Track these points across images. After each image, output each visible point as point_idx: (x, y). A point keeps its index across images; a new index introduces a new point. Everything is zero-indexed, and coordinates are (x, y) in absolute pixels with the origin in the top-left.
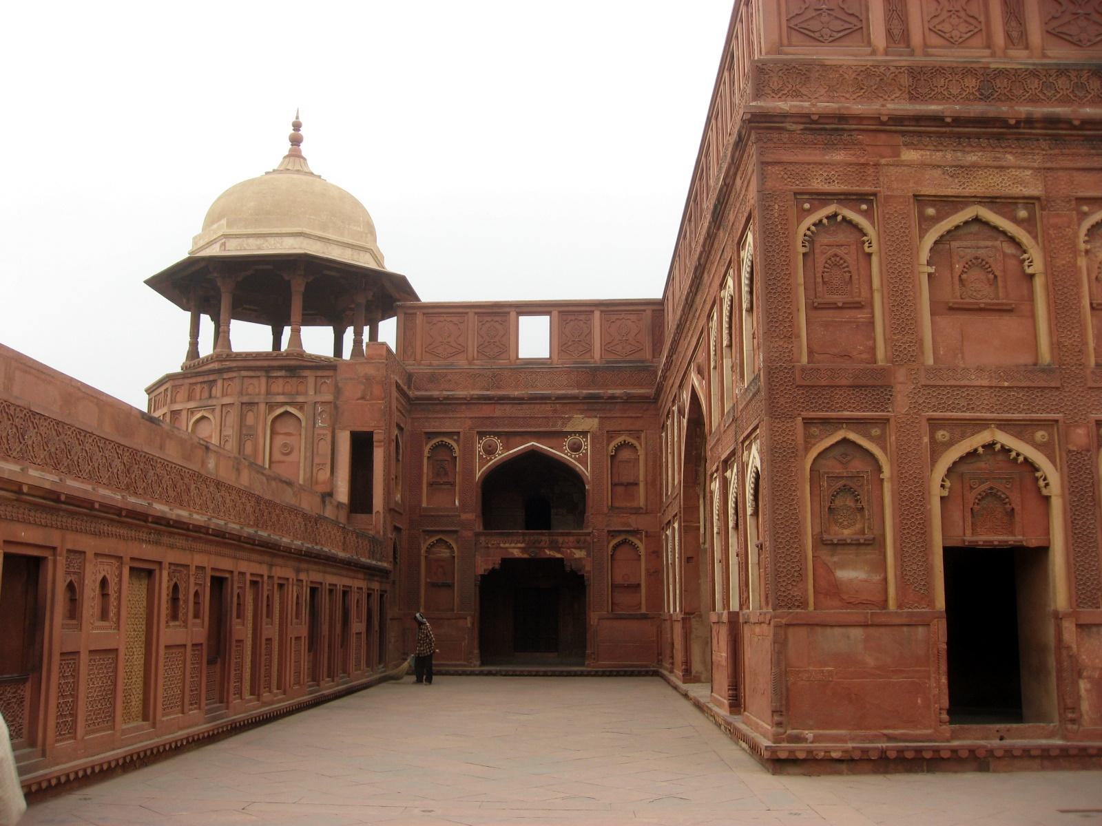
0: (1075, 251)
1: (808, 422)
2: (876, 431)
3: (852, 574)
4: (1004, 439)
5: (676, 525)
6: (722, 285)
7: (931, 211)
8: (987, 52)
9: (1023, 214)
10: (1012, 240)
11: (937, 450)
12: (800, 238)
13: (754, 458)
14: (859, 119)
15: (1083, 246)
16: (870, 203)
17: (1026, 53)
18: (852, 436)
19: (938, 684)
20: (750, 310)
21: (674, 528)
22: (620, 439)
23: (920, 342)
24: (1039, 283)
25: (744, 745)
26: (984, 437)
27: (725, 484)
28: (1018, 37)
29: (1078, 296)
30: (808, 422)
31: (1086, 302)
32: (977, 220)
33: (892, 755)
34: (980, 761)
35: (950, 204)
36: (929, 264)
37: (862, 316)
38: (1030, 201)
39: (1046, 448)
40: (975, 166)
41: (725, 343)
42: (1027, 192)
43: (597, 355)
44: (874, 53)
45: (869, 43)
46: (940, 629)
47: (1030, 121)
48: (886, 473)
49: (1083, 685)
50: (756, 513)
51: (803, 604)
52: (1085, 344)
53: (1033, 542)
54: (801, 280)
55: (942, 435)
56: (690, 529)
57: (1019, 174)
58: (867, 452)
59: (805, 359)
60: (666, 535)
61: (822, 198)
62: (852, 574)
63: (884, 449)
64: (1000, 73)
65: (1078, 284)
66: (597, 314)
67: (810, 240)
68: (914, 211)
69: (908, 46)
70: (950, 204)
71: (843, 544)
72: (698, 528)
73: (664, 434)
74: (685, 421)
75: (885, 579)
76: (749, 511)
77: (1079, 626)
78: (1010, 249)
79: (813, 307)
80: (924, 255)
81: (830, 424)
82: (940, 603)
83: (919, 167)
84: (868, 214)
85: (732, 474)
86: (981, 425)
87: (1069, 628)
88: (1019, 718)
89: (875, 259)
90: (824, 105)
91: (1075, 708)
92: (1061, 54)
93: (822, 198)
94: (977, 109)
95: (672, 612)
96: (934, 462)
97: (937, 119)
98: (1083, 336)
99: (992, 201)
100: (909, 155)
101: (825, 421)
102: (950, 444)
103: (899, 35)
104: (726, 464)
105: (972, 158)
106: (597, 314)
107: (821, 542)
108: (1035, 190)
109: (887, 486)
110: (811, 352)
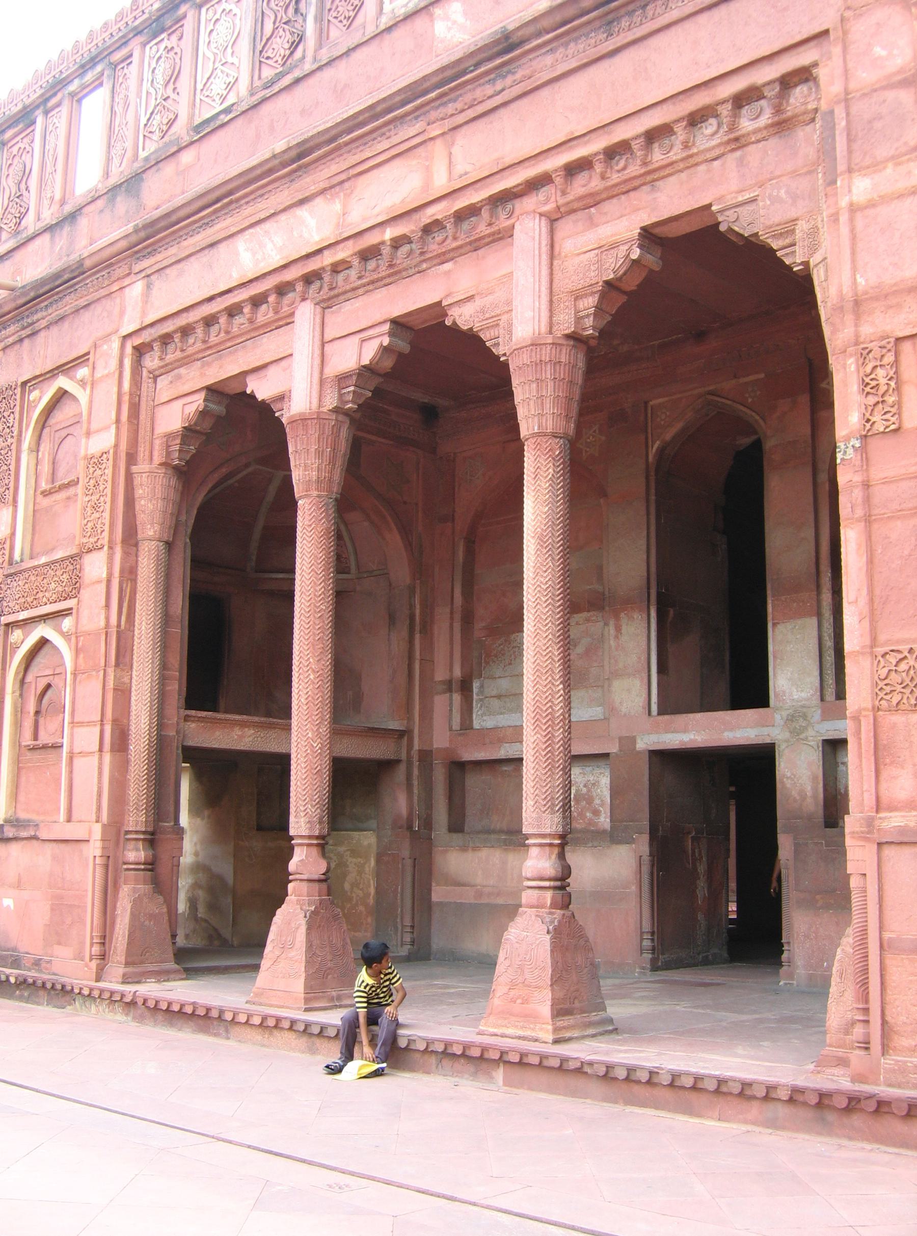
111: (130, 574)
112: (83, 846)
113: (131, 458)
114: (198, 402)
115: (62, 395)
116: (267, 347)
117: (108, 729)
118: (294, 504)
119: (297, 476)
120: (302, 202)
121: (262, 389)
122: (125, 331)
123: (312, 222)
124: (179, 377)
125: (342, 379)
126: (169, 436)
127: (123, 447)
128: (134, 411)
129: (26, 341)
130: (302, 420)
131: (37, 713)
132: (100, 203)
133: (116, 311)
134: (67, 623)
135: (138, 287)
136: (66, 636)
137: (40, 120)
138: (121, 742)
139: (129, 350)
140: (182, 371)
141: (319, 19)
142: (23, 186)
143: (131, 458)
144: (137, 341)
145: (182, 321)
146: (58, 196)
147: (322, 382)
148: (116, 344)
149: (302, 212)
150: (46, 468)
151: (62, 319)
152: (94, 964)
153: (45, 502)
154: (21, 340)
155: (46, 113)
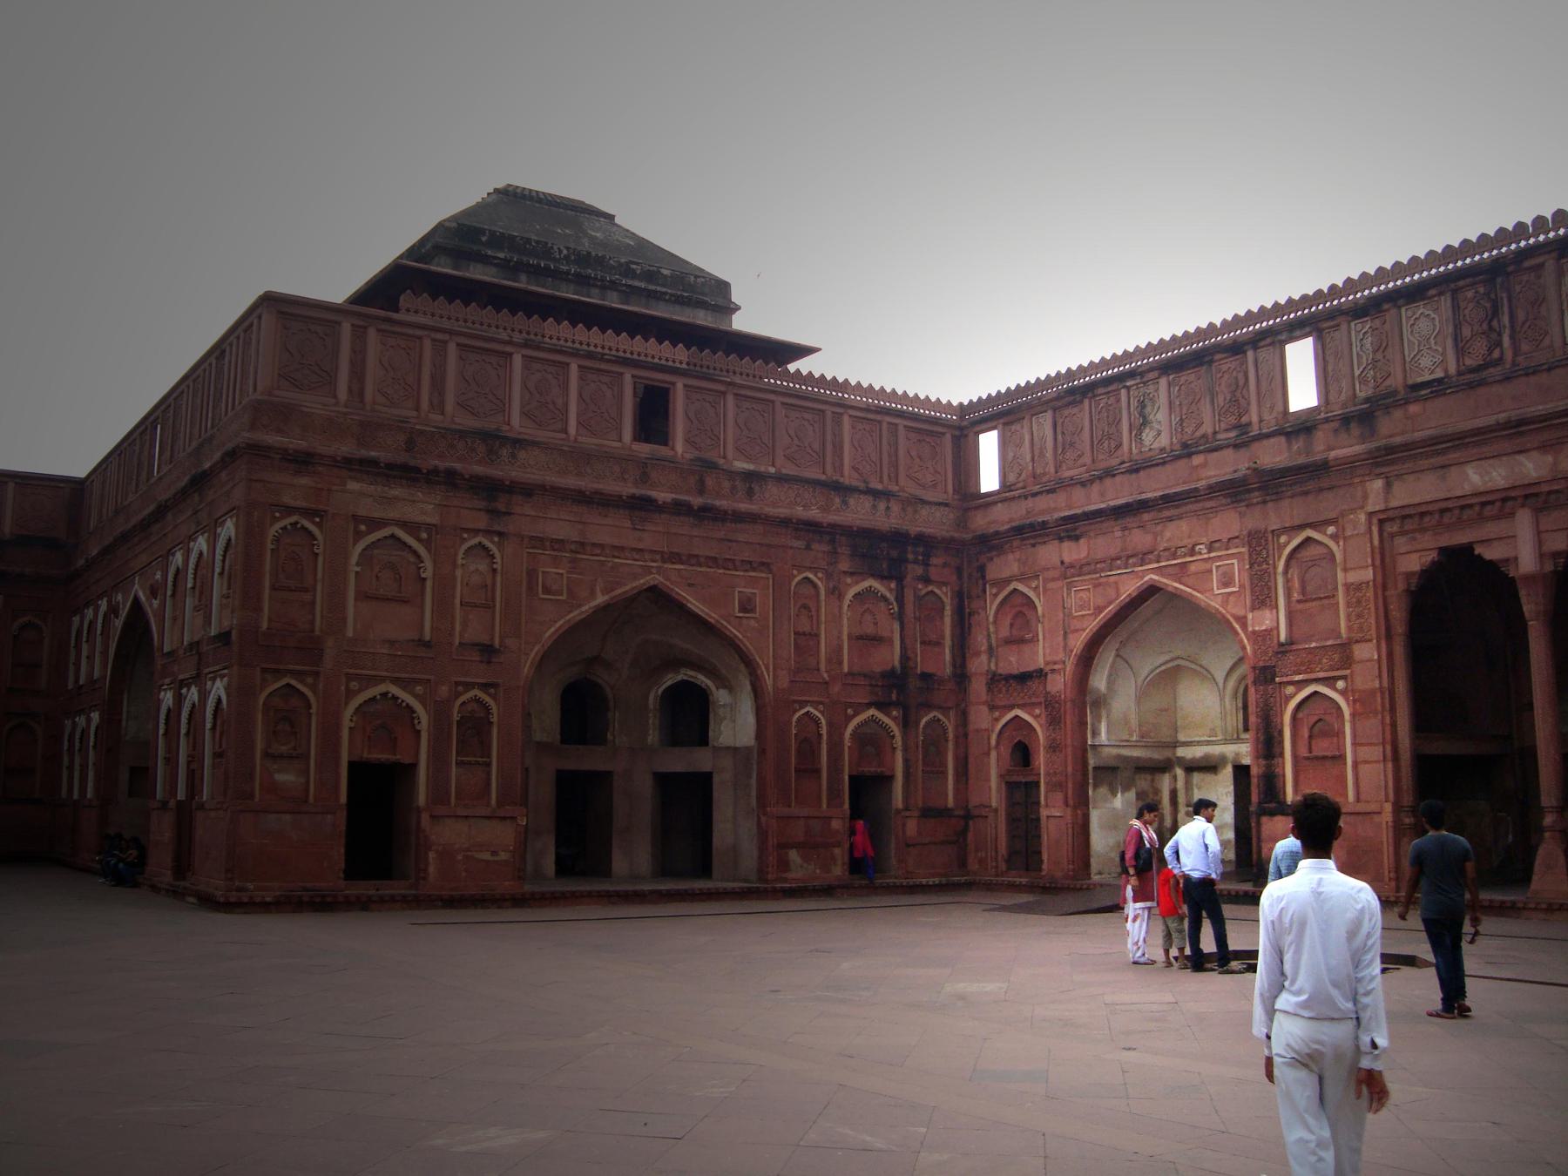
0: (454, 565)
1: (264, 670)
2: (310, 680)
3: (286, 777)
4: (395, 690)
5: (95, 716)
6: (192, 538)
7: (363, 528)
8: (414, 414)
9: (424, 535)
10: (415, 553)
11: (350, 694)
12: (270, 538)
13: (218, 689)
14: (322, 456)
15: (460, 562)
16: (321, 517)
17: (440, 417)
18: (293, 682)
19: (338, 853)
20: (221, 574)
21: (89, 720)
22: (26, 619)
23: (344, 620)
24: (429, 584)
25: (191, 899)
26: (382, 688)
27: (179, 699)
28: (439, 406)
29: (453, 596)
30: (264, 670)
31: (457, 601)
32: (393, 536)
33: (305, 899)
34: (364, 905)
35: (375, 524)
36: (358, 564)
37: (307, 597)
38: (429, 527)
39: (421, 699)
40: (396, 498)
41: (190, 585)
42: (429, 520)
43: (7, 530)
44: (337, 404)
45: (335, 397)
46: (342, 817)
47: (436, 471)
48: (313, 710)
49: (431, 855)
50: (214, 728)
51: (252, 796)
52: (453, 628)
53: (407, 761)
54: (268, 567)
55: (354, 685)
56: (112, 719)
57: (423, 506)
58: (302, 694)
59: (265, 625)
60: (75, 725)
61: (289, 510)
62: (286, 777)
63: (315, 693)
64: (422, 432)
65: (454, 587)
66: (11, 485)
67: (277, 540)
68: (351, 527)
69: (362, 401)
70: (375, 524)
71: (281, 756)
72: (120, 721)
73: (76, 619)
74: (118, 623)
75: (308, 782)
76: (208, 725)
77: (432, 817)
78: (412, 559)
79: (273, 588)
80: (354, 559)
81: (278, 673)
82: (343, 799)
83: (358, 494)
84: (319, 525)
85: (193, 694)
86: (383, 680)
87: (425, 817)
88: (390, 878)
89: (320, 559)
90: (295, 442)
91: (425, 870)
92: (468, 422)
93: (289, 510)
94: (402, 458)
95: (76, 796)
96: (346, 704)
97: (374, 463)
98: (453, 623)
99: (404, 525)
100: (353, 485)
101: (277, 671)
102: (360, 691)
103: (357, 392)
104: (184, 683)
105: (396, 492)
106: (11, 485)
107: (267, 755)
108: (434, 520)
109: (314, 719)
110: (270, 620)
111: (1390, 655)
112: (1376, 818)
113: (1385, 588)
114: (1433, 555)
115: (1308, 540)
116: (1491, 529)
117: (1389, 748)
118: (1526, 625)
119: (1525, 608)
120: (1520, 452)
121: (1490, 553)
122: (1370, 508)
123: (1530, 466)
124: (1414, 539)
125: (1555, 555)
126: (1409, 575)
127: (1379, 578)
128: (1384, 560)
129: (1270, 505)
130: (1529, 579)
131: (1310, 737)
132: (1333, 425)
133: (1359, 494)
134: (1340, 684)
135: (1379, 484)
136: (1343, 693)
137: (1250, 354)
138: (1396, 758)
139: (1375, 521)
140: (1418, 535)
141: (1512, 337)
142: (1238, 394)
143: (1385, 588)
144: (1382, 516)
145: (1424, 509)
146: (1281, 409)
147: (1542, 556)
148: (1363, 517)
149: (1521, 458)
150: (1297, 584)
151: (1306, 493)
152: (1393, 884)
153: (1300, 606)
154: (1264, 502)
155: (1255, 348)
